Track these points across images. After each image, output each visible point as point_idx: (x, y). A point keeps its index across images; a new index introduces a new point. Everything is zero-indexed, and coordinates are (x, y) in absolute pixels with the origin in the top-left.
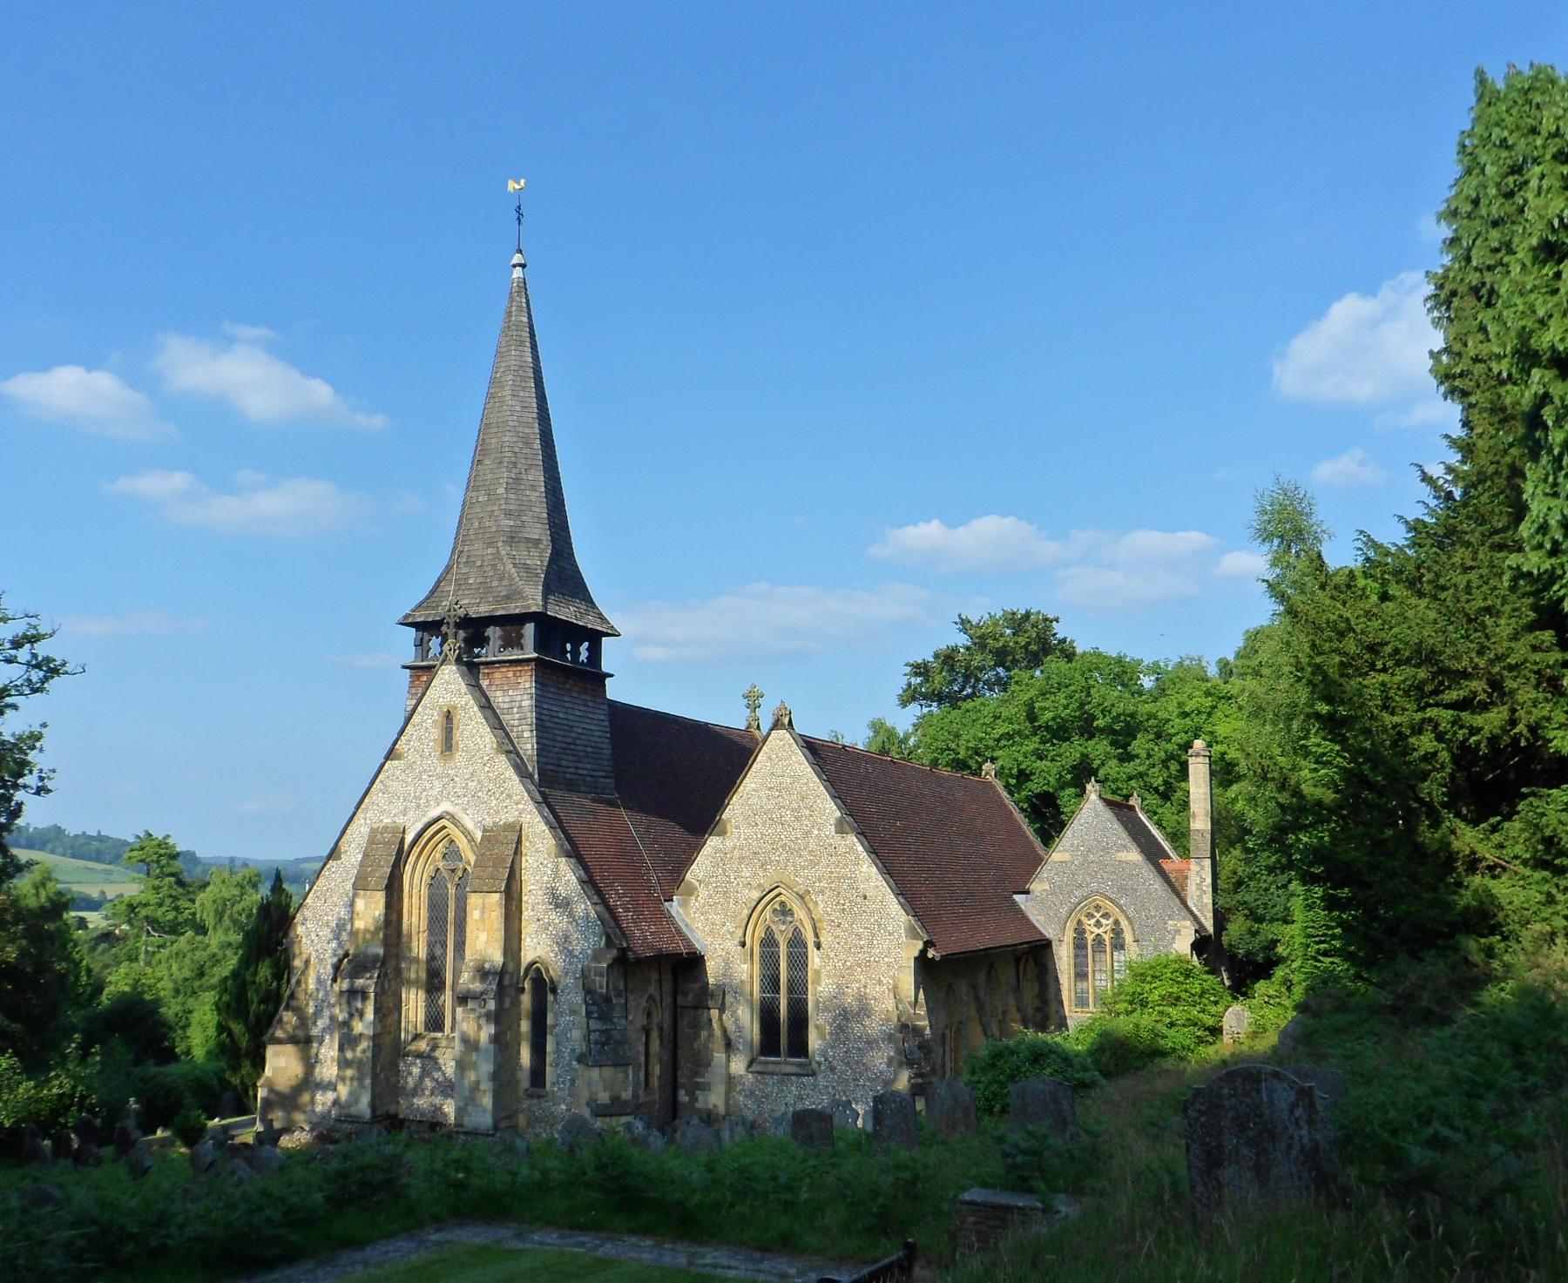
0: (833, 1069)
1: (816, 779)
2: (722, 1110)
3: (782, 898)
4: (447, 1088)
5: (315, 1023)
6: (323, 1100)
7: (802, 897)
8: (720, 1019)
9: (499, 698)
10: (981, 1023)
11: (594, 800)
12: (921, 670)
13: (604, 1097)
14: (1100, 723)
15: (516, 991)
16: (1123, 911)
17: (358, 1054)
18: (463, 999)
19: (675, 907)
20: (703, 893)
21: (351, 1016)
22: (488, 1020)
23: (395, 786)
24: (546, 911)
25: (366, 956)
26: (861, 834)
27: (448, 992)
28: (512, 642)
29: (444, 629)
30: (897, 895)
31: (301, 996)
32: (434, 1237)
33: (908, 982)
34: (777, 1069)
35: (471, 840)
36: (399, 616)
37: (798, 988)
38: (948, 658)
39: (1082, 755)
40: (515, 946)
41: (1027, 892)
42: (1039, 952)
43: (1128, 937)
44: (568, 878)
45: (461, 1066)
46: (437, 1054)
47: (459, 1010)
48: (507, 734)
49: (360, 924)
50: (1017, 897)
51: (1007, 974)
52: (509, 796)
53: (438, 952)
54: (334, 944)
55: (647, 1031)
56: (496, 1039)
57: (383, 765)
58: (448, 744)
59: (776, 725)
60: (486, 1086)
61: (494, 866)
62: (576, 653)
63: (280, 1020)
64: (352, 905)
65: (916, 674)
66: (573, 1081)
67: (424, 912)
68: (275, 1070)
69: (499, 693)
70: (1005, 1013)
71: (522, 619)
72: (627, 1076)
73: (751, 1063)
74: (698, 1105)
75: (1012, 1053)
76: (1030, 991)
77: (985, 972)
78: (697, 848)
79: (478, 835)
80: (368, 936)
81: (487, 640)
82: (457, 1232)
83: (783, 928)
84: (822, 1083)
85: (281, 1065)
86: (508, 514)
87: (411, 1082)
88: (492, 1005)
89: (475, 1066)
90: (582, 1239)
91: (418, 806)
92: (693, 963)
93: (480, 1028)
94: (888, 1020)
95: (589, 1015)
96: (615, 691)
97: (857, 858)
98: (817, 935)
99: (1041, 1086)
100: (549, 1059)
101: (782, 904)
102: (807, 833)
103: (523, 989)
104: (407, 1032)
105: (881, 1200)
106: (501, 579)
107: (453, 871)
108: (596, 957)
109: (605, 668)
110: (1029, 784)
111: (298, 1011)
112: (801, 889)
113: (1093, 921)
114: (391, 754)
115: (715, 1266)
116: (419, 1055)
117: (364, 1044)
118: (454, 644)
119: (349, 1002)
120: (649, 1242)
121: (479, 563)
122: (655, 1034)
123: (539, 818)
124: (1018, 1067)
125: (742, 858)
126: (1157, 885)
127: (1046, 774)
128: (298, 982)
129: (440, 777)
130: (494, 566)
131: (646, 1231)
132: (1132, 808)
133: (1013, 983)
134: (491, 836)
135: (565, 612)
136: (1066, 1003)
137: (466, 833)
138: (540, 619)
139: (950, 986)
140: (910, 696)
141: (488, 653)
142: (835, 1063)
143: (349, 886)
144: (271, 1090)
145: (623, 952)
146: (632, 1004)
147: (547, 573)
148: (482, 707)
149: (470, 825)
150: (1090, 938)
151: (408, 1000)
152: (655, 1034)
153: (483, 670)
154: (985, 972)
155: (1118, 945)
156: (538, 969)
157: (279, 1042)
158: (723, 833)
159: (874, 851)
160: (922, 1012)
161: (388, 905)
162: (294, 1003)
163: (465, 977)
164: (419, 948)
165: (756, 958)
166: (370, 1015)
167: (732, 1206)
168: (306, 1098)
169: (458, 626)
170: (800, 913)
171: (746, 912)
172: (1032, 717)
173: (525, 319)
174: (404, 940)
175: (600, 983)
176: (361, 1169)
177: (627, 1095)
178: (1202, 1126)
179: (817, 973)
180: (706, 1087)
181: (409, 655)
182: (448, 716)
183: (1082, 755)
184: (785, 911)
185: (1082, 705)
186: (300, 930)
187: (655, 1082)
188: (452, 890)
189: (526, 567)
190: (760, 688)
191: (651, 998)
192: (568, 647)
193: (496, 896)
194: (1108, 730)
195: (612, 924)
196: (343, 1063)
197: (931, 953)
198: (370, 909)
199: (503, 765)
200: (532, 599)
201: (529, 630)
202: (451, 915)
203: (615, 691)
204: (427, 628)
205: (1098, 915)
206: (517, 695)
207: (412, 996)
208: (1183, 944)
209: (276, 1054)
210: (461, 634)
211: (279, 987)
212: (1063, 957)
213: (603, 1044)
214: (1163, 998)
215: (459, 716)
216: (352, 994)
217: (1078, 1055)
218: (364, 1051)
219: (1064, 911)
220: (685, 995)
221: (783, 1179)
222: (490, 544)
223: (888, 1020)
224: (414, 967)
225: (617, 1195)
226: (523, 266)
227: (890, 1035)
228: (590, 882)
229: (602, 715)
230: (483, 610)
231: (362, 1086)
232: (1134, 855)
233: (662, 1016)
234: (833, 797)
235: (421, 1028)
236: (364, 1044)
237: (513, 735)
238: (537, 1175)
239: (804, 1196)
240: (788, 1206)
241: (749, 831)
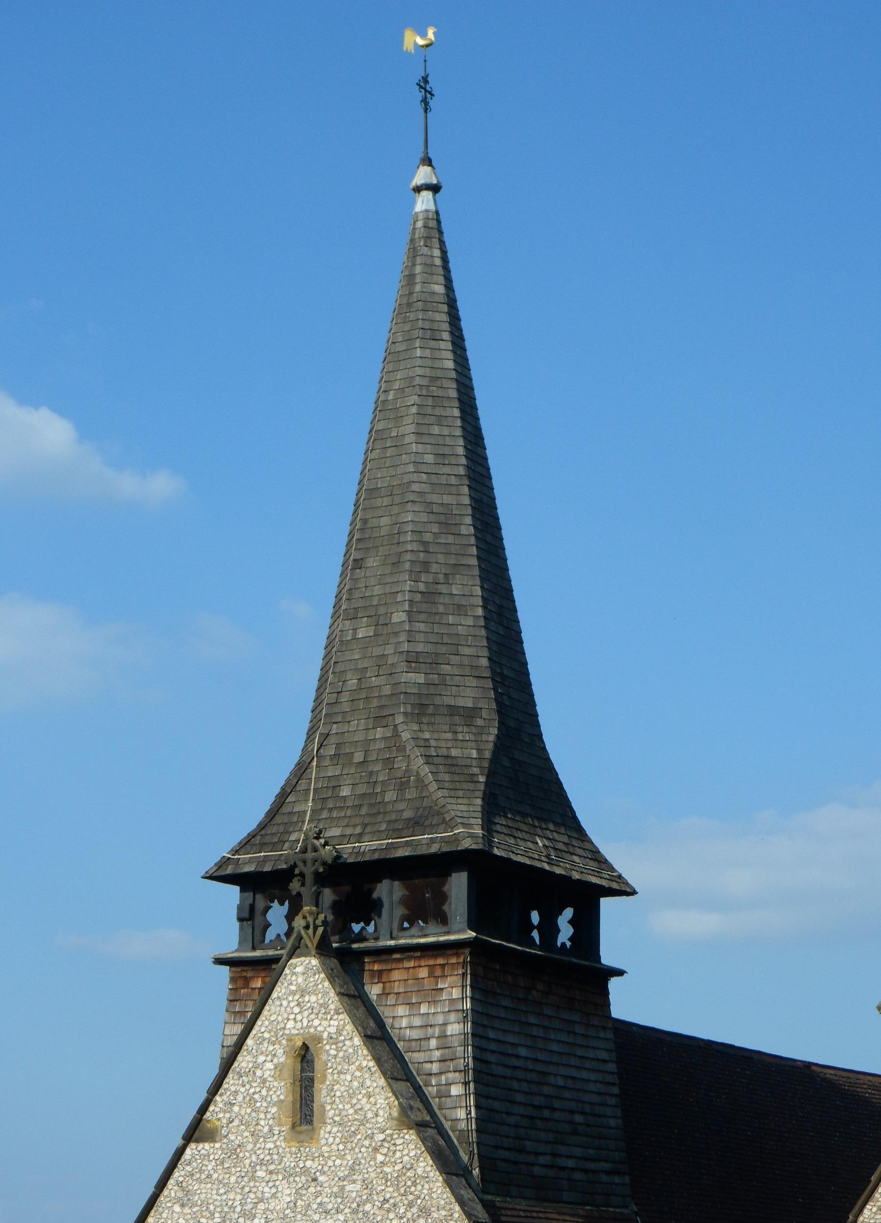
9: (402, 1020)
23: (202, 1191)
28: (426, 908)
29: (295, 886)
36: (209, 863)
58: (304, 1112)
62: (549, 929)
69: (401, 1010)
71: (440, 865)
96: (627, 1003)
106: (402, 786)
109: (608, 958)
114: (197, 1131)
118: (313, 917)
121: (359, 757)
129: (288, 1175)
130: (389, 762)
135: (529, 849)
141: (381, 932)
148: (368, 1038)
173: (440, 289)
182: (305, 1056)
189: (451, 764)
192: (535, 917)
199: (410, 1147)
200: (464, 827)
201: (458, 885)
203: (627, 1003)
206: (437, 1013)
215: (326, 1054)
222: (380, 720)
230: (370, 846)
237: (430, 1091)
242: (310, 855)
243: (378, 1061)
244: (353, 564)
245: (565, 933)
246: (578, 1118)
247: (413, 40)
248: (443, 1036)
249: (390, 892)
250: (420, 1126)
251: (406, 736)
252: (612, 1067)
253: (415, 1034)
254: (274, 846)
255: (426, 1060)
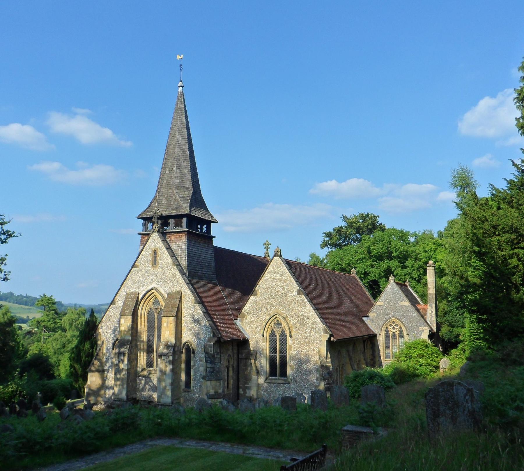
0: (296, 382)
1: (290, 275)
2: (255, 396)
3: (278, 319)
4: (154, 389)
5: (106, 365)
6: (109, 393)
7: (285, 318)
8: (255, 363)
9: (173, 245)
10: (351, 365)
11: (208, 283)
12: (329, 235)
13: (212, 392)
14: (394, 254)
15: (180, 352)
16: (403, 323)
17: (122, 376)
18: (160, 356)
19: (238, 322)
20: (248, 317)
21: (119, 362)
22: (170, 364)
23: (136, 278)
24: (191, 324)
25: (125, 340)
26: (307, 295)
27: (155, 353)
28: (178, 224)
29: (153, 220)
30: (320, 318)
31: (101, 355)
32: (149, 443)
33: (324, 349)
34: (276, 381)
35: (163, 297)
36: (137, 216)
37: (283, 352)
38: (339, 231)
39: (388, 266)
40: (180, 337)
41: (368, 317)
42: (372, 338)
43: (405, 333)
44: (199, 311)
45: (160, 380)
46: (151, 376)
47: (159, 360)
48: (176, 259)
49: (122, 328)
50: (364, 319)
51: (360, 347)
52: (177, 281)
53: (151, 338)
54: (113, 336)
55: (228, 368)
56: (172, 370)
57: (131, 270)
58: (155, 262)
59: (275, 255)
60: (169, 388)
61: (172, 307)
62: (202, 229)
63: (93, 364)
64: (119, 321)
65: (327, 237)
66: (201, 386)
67: (146, 324)
68: (91, 382)
69: (173, 244)
70: (359, 361)
71: (182, 216)
72: (220, 384)
73: (266, 379)
74: (247, 395)
75: (362, 375)
76: (369, 353)
77: (352, 346)
78: (246, 300)
79: (166, 296)
80: (125, 333)
81: (169, 224)
82: (158, 441)
83: (278, 330)
84: (292, 386)
85: (93, 380)
86: (177, 178)
87: (141, 386)
88: (171, 358)
89: (164, 380)
90: (204, 444)
91: (144, 285)
92: (245, 342)
93: (166, 366)
94: (317, 363)
95: (206, 361)
96: (216, 243)
97: (305, 304)
98: (290, 332)
99: (373, 387)
100: (192, 378)
101: (278, 321)
102: (287, 295)
103: (182, 352)
104: (140, 368)
105: (314, 430)
106: (174, 202)
107: (157, 309)
108: (209, 340)
109: (213, 234)
110: (368, 277)
111: (100, 360)
112: (285, 315)
113: (392, 327)
114: (134, 266)
115: (253, 454)
116: (144, 376)
117: (124, 372)
118: (157, 225)
119: (118, 357)
120: (228, 445)
121: (166, 196)
122: (231, 369)
123: (188, 289)
124: (364, 381)
125: (263, 304)
126: (415, 314)
127: (375, 273)
128: (100, 350)
129: (152, 274)
130: (172, 197)
131: (228, 441)
132: (406, 286)
133: (362, 349)
134: (171, 296)
135: (198, 214)
136: (382, 357)
137: (161, 294)
138: (189, 217)
139: (339, 351)
140: (325, 245)
141: (169, 229)
142: (297, 379)
143: (118, 314)
144: (90, 389)
145: (219, 338)
146: (222, 358)
147: (191, 200)
148: (167, 249)
149: (163, 292)
150: (391, 333)
151: (140, 356)
152: (231, 369)
153: (168, 235)
154: (352, 346)
155: (401, 336)
156: (188, 345)
157: (93, 371)
158: (256, 295)
159: (311, 301)
160: (329, 360)
161: (133, 321)
162: (98, 357)
163: (161, 347)
164: (144, 337)
165: (268, 341)
166: (126, 362)
167: (259, 432)
168: (102, 392)
169: (158, 219)
170: (284, 324)
171: (264, 324)
172: (369, 252)
173: (183, 106)
174: (139, 334)
175: (211, 350)
176: (123, 418)
177: (220, 391)
178: (432, 402)
179: (291, 346)
180: (250, 388)
181: (141, 230)
182: (155, 252)
183: (388, 266)
184: (278, 324)
185: (388, 248)
186: (100, 330)
187: (231, 386)
188: (156, 316)
190: (269, 242)
191: (229, 356)
192: (199, 226)
193: (173, 318)
194: (397, 257)
195: (215, 328)
196: (116, 379)
197: (332, 339)
198: (126, 323)
199: (175, 269)
200: (186, 209)
201: (185, 220)
202: (156, 325)
203: (216, 243)
204: (147, 220)
205: (394, 325)
206: (180, 244)
207: (142, 355)
208: (425, 336)
209: (92, 376)
210: (160, 222)
211: (93, 351)
212: (381, 340)
213: (212, 372)
214: (417, 355)
215: (159, 252)
216: (120, 354)
217: (386, 376)
218: (124, 375)
219: (381, 323)
220: (242, 354)
221: (278, 422)
222: (170, 189)
223: (317, 363)
224: (142, 344)
225: (217, 427)
226: (182, 87)
227: (317, 369)
228: (207, 313)
229: (211, 251)
230: (168, 213)
231: (123, 388)
232: (407, 303)
233: (233, 362)
234: (296, 282)
235: (145, 367)
236: (124, 372)
237: (179, 259)
238: (187, 420)
239: (286, 428)
240: (280, 432)
241: (266, 294)
242: (156, 214)
243: (169, 253)
244: (166, 159)
245: (205, 230)
246: (207, 264)
247: (178, 57)
248: (181, 248)
249: (171, 221)
250: (177, 265)
251: (175, 192)
252: (213, 255)
253: (176, 248)
254: (149, 212)
255: (178, 253)
